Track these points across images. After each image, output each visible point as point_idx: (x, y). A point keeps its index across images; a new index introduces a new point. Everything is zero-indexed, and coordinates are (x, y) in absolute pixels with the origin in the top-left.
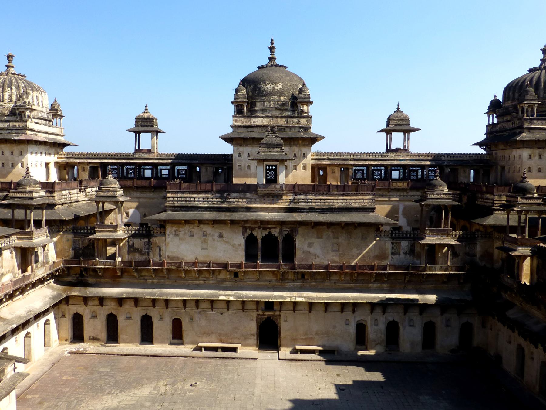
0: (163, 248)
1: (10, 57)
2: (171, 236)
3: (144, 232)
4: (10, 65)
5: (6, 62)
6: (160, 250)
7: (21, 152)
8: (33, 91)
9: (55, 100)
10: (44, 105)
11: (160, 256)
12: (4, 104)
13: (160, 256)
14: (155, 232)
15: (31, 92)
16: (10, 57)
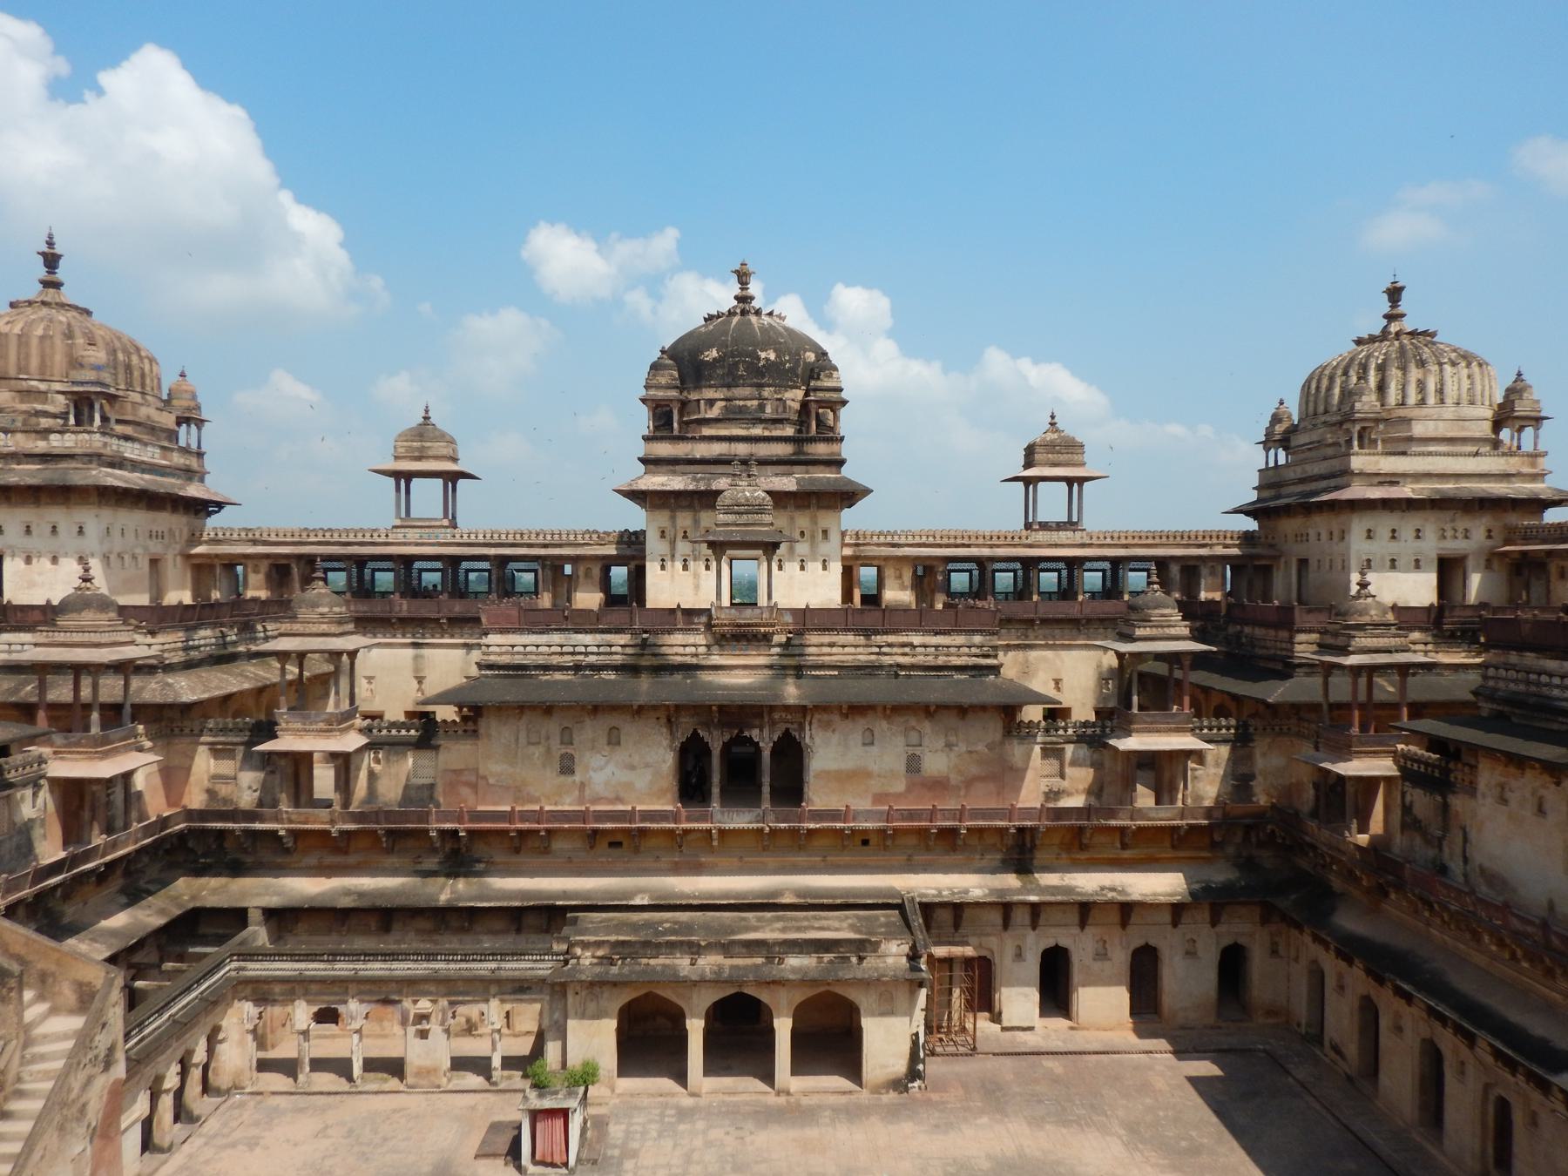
0: (1473, 835)
1: (1394, 294)
2: (1489, 800)
3: (1437, 774)
4: (1395, 311)
5: (1385, 307)
6: (1466, 840)
7: (1343, 532)
8: (1404, 369)
9: (1519, 374)
10: (1449, 400)
11: (1466, 860)
12: (1329, 419)
13: (1466, 860)
14: (1460, 777)
15: (1399, 373)
16: (1394, 294)
